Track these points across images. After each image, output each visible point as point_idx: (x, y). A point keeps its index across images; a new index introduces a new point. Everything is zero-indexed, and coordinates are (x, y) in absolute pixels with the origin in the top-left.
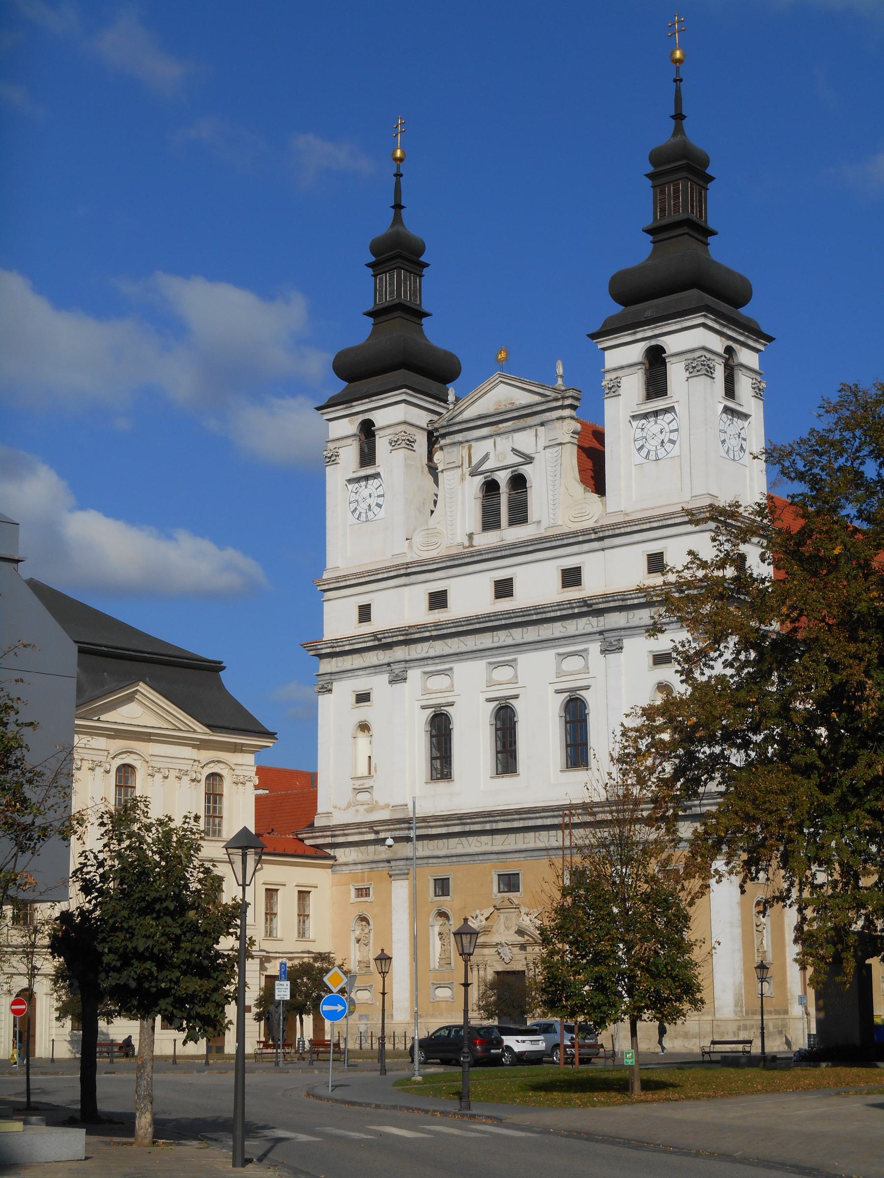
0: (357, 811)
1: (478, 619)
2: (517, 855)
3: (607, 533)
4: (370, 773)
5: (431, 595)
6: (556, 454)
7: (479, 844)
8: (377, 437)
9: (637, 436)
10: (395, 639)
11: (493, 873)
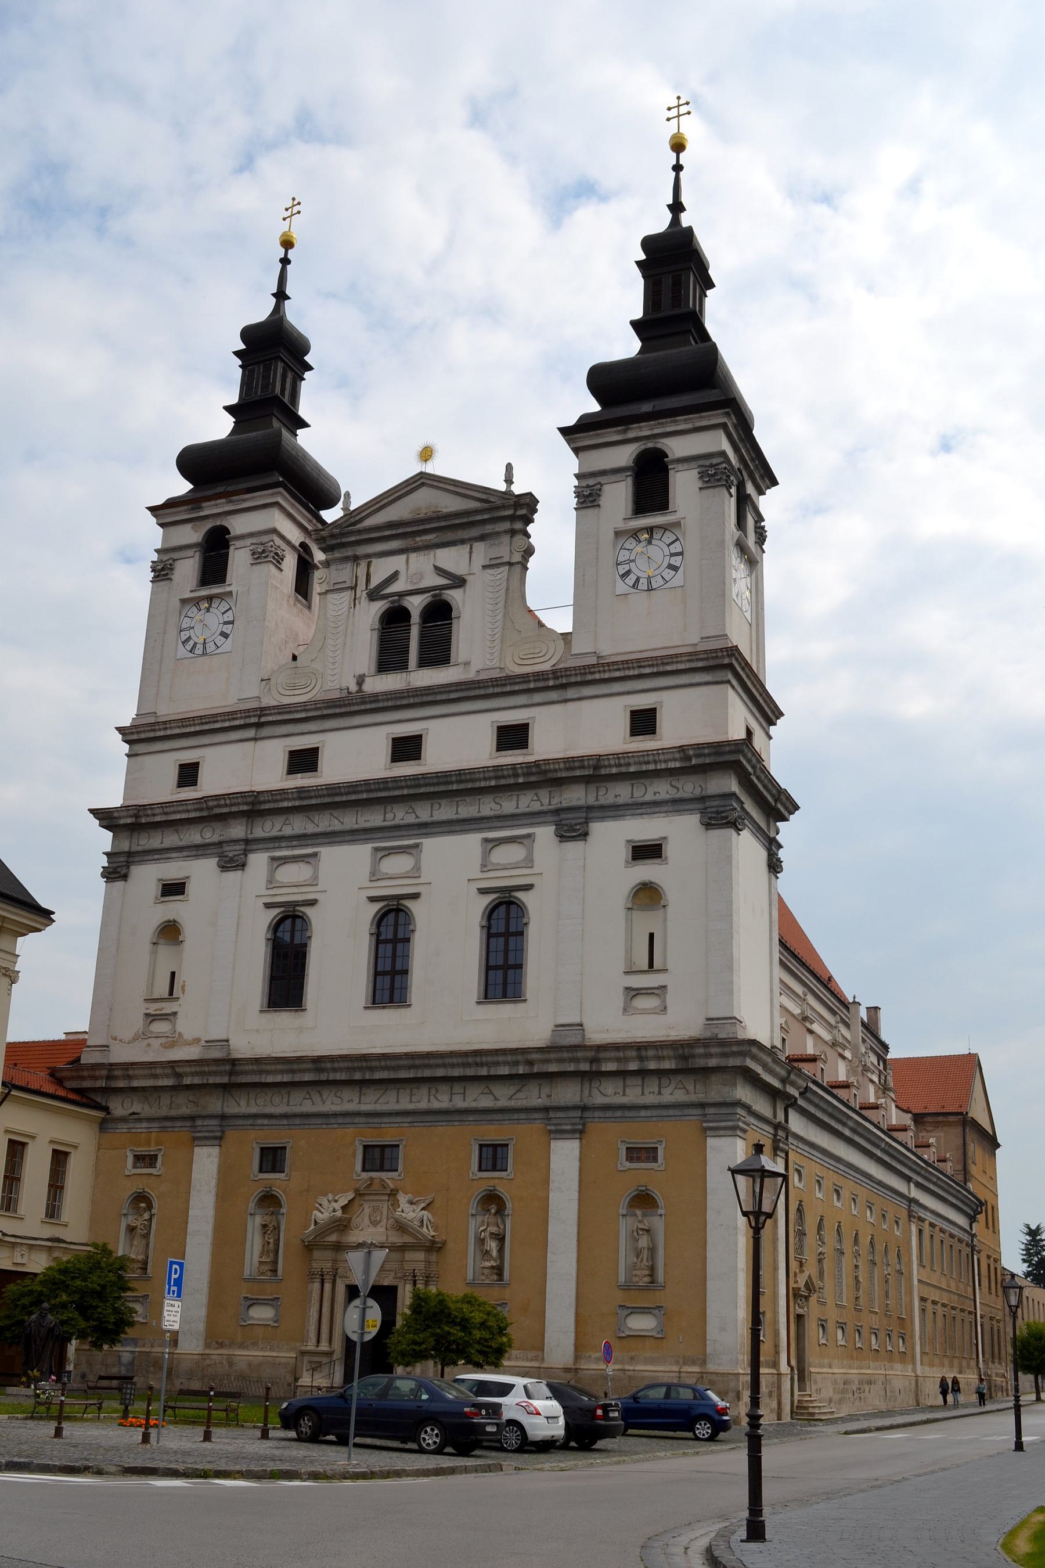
0: (149, 1045)
1: (366, 785)
2: (399, 1119)
3: (573, 680)
4: (171, 993)
5: (292, 753)
6: (499, 577)
7: (339, 1101)
8: (232, 548)
9: (621, 559)
10: (234, 809)
11: (357, 1143)
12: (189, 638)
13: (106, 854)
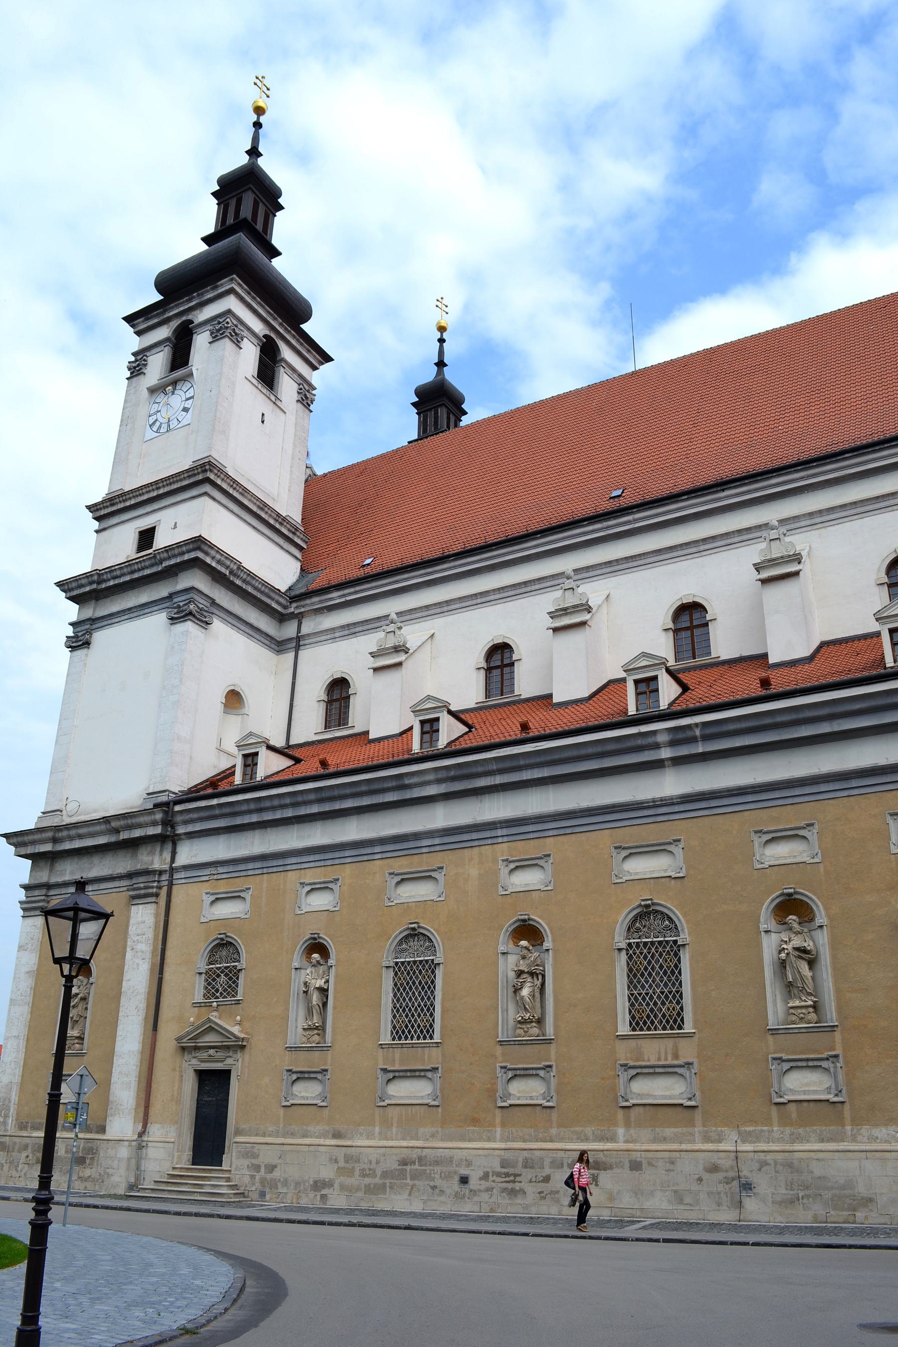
12: (156, 420)
13: (71, 624)
